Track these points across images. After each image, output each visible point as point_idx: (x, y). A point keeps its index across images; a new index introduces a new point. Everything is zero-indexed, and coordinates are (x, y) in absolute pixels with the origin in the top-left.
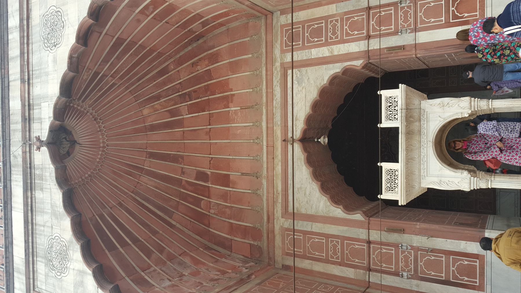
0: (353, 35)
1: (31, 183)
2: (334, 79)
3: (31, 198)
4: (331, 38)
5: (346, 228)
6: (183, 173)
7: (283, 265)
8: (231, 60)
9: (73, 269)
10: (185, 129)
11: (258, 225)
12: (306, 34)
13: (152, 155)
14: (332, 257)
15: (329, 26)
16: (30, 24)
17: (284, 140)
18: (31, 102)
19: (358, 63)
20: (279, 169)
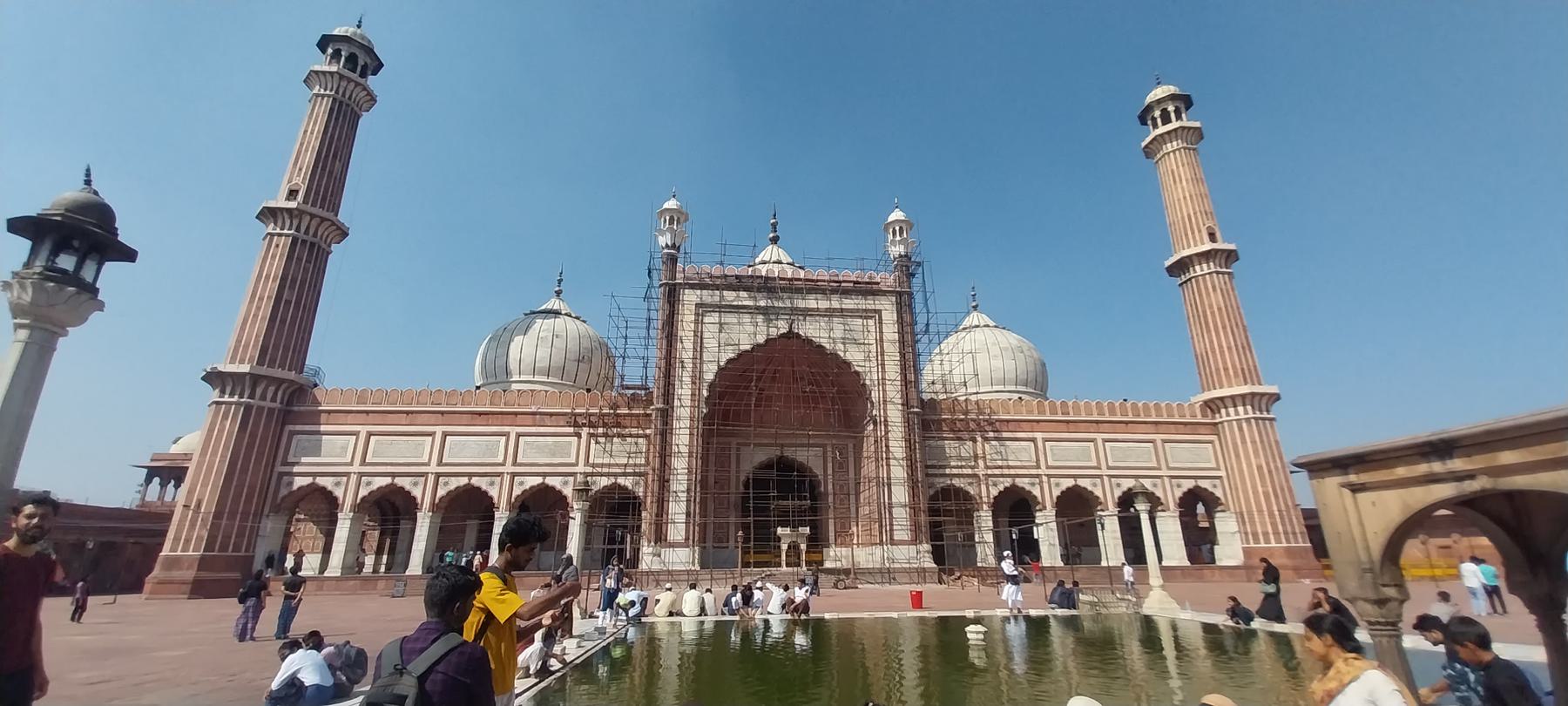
19: (822, 489)
20: (766, 441)
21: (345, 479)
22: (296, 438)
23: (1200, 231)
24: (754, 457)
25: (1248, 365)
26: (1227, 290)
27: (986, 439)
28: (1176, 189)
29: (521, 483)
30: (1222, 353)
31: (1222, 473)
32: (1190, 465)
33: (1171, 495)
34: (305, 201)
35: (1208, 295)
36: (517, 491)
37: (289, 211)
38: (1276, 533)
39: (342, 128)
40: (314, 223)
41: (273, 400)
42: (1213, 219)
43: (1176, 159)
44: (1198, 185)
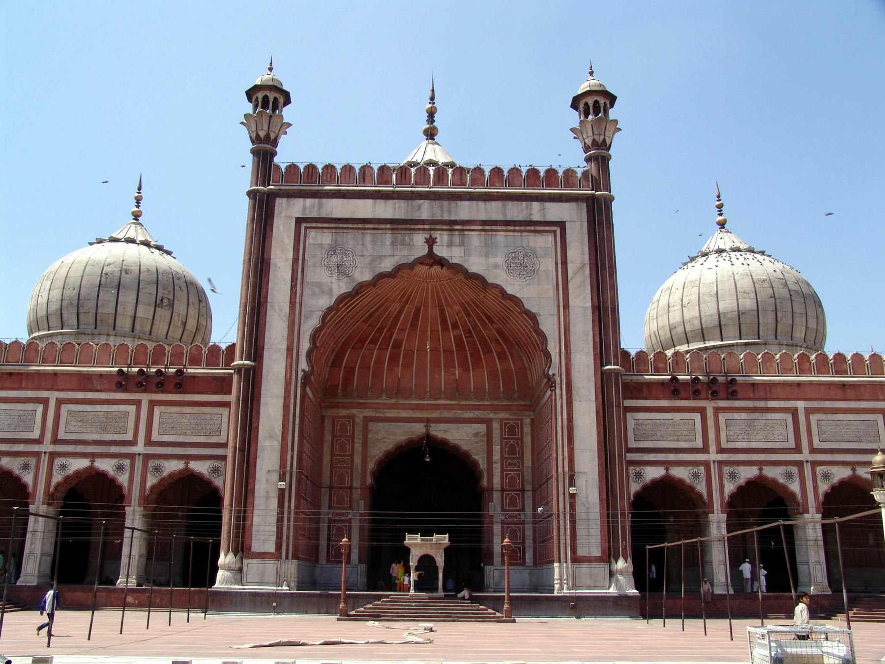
0: (506, 479)
1: (397, 229)
2: (475, 464)
3: (385, 229)
4: (506, 462)
5: (360, 470)
6: (401, 330)
7: (324, 416)
8: (500, 371)
9: (332, 282)
10: (440, 334)
11: (355, 394)
12: (512, 441)
13: (418, 310)
14: (336, 459)
15: (515, 461)
16: (531, 234)
17: (428, 420)
18: (466, 233)
19: (485, 482)
20: (404, 414)
27: (717, 410)
29: (63, 467)
36: (57, 478)
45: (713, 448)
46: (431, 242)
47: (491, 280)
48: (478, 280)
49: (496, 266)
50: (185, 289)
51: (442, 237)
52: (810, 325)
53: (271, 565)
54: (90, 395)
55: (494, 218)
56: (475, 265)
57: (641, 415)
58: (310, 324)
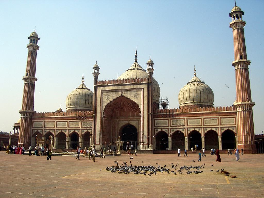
2: (136, 128)
19: (138, 132)
20: (124, 120)
21: (42, 130)
22: (34, 123)
23: (238, 55)
24: (122, 123)
25: (244, 96)
26: (243, 73)
27: (171, 119)
28: (234, 41)
30: (239, 92)
31: (236, 126)
32: (227, 124)
33: (219, 132)
34: (29, 76)
35: (238, 74)
37: (27, 78)
38: (243, 142)
39: (34, 57)
40: (31, 79)
41: (29, 116)
42: (242, 51)
43: (235, 32)
44: (240, 41)
45: (170, 126)
46: (122, 93)
47: (131, 99)
48: (129, 99)
49: (132, 97)
50: (91, 97)
51: (124, 92)
52: (205, 98)
53: (99, 146)
54: (73, 120)
55: (132, 88)
56: (129, 97)
57: (158, 120)
58: (104, 108)
